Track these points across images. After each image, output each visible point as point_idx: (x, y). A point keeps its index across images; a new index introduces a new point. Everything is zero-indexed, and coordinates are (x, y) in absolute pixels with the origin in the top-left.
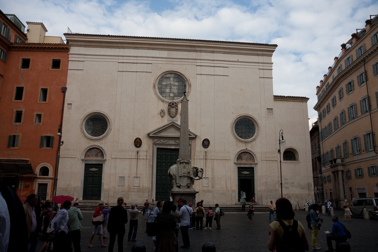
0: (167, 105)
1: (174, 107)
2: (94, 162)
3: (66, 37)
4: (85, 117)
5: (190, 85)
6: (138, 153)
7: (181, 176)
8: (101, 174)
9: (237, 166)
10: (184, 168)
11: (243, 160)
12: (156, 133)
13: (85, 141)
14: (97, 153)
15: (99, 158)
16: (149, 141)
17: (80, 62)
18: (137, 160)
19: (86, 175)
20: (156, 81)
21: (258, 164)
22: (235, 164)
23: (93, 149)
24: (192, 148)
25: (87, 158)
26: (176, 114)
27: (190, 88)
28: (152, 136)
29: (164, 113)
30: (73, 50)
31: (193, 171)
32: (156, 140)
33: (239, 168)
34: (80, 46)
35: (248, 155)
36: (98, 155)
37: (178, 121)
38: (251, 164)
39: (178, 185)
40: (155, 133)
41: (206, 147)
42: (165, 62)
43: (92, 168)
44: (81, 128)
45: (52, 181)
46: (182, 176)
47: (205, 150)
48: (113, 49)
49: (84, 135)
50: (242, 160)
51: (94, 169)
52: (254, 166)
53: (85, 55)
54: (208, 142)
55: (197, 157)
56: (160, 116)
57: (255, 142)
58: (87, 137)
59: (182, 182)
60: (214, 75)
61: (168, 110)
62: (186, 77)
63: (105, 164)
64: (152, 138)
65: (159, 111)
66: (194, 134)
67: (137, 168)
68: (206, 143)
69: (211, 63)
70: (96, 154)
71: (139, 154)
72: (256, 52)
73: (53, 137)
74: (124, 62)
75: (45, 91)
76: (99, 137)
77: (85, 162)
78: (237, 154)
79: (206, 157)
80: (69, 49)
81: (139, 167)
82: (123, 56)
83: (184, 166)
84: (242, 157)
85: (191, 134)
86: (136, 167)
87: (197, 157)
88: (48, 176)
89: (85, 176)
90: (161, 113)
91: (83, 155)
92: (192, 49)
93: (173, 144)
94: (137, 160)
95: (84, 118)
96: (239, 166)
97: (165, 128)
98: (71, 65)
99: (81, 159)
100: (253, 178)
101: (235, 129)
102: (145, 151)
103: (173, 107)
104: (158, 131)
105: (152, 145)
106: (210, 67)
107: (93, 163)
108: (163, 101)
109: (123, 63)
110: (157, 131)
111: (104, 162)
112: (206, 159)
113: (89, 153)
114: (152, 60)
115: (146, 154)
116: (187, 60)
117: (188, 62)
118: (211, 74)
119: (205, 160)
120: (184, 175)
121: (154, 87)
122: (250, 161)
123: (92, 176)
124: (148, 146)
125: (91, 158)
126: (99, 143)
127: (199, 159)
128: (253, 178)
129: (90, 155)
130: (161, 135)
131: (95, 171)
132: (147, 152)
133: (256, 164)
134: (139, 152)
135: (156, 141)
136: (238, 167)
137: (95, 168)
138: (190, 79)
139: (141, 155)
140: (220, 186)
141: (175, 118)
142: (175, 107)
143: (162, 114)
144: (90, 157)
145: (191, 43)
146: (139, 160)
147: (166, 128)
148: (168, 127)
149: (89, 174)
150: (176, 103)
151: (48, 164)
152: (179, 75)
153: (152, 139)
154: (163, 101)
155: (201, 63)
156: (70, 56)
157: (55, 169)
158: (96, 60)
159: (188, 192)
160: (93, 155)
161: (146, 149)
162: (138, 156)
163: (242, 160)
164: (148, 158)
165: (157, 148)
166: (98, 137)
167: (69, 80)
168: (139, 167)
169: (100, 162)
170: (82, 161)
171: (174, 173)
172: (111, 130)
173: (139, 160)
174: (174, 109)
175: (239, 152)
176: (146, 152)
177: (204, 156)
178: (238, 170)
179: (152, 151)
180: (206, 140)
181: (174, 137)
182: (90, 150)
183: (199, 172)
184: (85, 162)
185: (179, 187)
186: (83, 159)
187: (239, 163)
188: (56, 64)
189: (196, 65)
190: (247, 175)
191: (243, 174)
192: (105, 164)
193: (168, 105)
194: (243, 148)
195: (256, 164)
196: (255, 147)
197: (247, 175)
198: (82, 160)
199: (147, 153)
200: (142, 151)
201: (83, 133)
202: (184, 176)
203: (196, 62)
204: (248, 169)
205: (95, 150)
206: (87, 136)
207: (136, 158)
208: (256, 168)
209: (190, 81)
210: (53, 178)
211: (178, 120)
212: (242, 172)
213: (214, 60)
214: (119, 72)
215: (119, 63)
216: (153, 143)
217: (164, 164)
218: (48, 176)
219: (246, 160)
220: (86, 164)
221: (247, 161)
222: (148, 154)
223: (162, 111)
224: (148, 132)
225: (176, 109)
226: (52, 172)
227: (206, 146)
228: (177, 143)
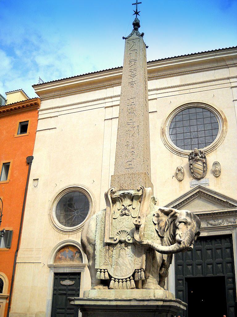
0: (186, 160)
1: (199, 160)
2: (67, 270)
3: (35, 90)
4: (55, 197)
5: (224, 121)
7: (109, 241)
8: (79, 290)
10: (125, 214)
13: (55, 234)
14: (73, 255)
15: (76, 263)
17: (52, 118)
19: (55, 292)
20: (165, 124)
23: (68, 248)
25: (58, 264)
26: (204, 171)
27: (226, 125)
29: (183, 173)
30: (44, 105)
31: (156, 222)
34: (53, 97)
36: (74, 258)
37: (210, 184)
39: (102, 277)
42: (177, 93)
43: (66, 279)
44: (50, 215)
45: (7, 302)
46: (113, 242)
48: (97, 91)
49: (54, 225)
51: (67, 282)
53: (59, 107)
56: (177, 180)
58: (56, 227)
59: (117, 264)
61: (190, 166)
62: (216, 109)
63: (84, 272)
65: (174, 171)
70: (72, 256)
73: (11, 232)
74: (113, 105)
75: (7, 166)
76: (77, 226)
77: (53, 270)
80: (38, 103)
82: (111, 97)
83: (125, 209)
88: (2, 293)
89: (54, 295)
90: (177, 174)
91: (51, 259)
92: (219, 64)
93: (204, 228)
95: (54, 199)
97: (186, 200)
98: (41, 125)
99: (48, 265)
103: (197, 160)
107: (66, 271)
108: (180, 153)
109: (112, 106)
111: (83, 269)
113: (61, 255)
116: (214, 83)
120: (123, 239)
121: (163, 133)
123: (65, 294)
125: (64, 262)
126: (75, 236)
129: (62, 257)
131: (70, 285)
137: (71, 279)
141: (202, 180)
142: (200, 160)
144: (62, 261)
145: (216, 55)
147: (188, 198)
148: (191, 197)
149: (60, 290)
150: (201, 153)
151: (3, 273)
152: (203, 108)
154: (179, 153)
156: (40, 113)
157: (11, 281)
158: (75, 111)
159: (130, 300)
160: (67, 257)
166: (74, 227)
167: (37, 145)
169: (77, 270)
170: (50, 267)
171: (88, 236)
172: (94, 213)
174: (199, 163)
181: (204, 213)
182: (62, 250)
183: (181, 226)
184: (53, 270)
185: (105, 283)
186: (51, 265)
188: (24, 128)
192: (85, 272)
193: (188, 159)
198: (50, 267)
201: (52, 222)
202: (121, 242)
203: (230, 83)
205: (71, 249)
206: (58, 226)
209: (223, 113)
210: (8, 296)
211: (209, 183)
214: (106, 121)
215: (106, 108)
217: (190, 267)
218: (2, 293)
220: (56, 274)
223: (179, 170)
225: (204, 163)
226: (7, 287)
228: (211, 225)
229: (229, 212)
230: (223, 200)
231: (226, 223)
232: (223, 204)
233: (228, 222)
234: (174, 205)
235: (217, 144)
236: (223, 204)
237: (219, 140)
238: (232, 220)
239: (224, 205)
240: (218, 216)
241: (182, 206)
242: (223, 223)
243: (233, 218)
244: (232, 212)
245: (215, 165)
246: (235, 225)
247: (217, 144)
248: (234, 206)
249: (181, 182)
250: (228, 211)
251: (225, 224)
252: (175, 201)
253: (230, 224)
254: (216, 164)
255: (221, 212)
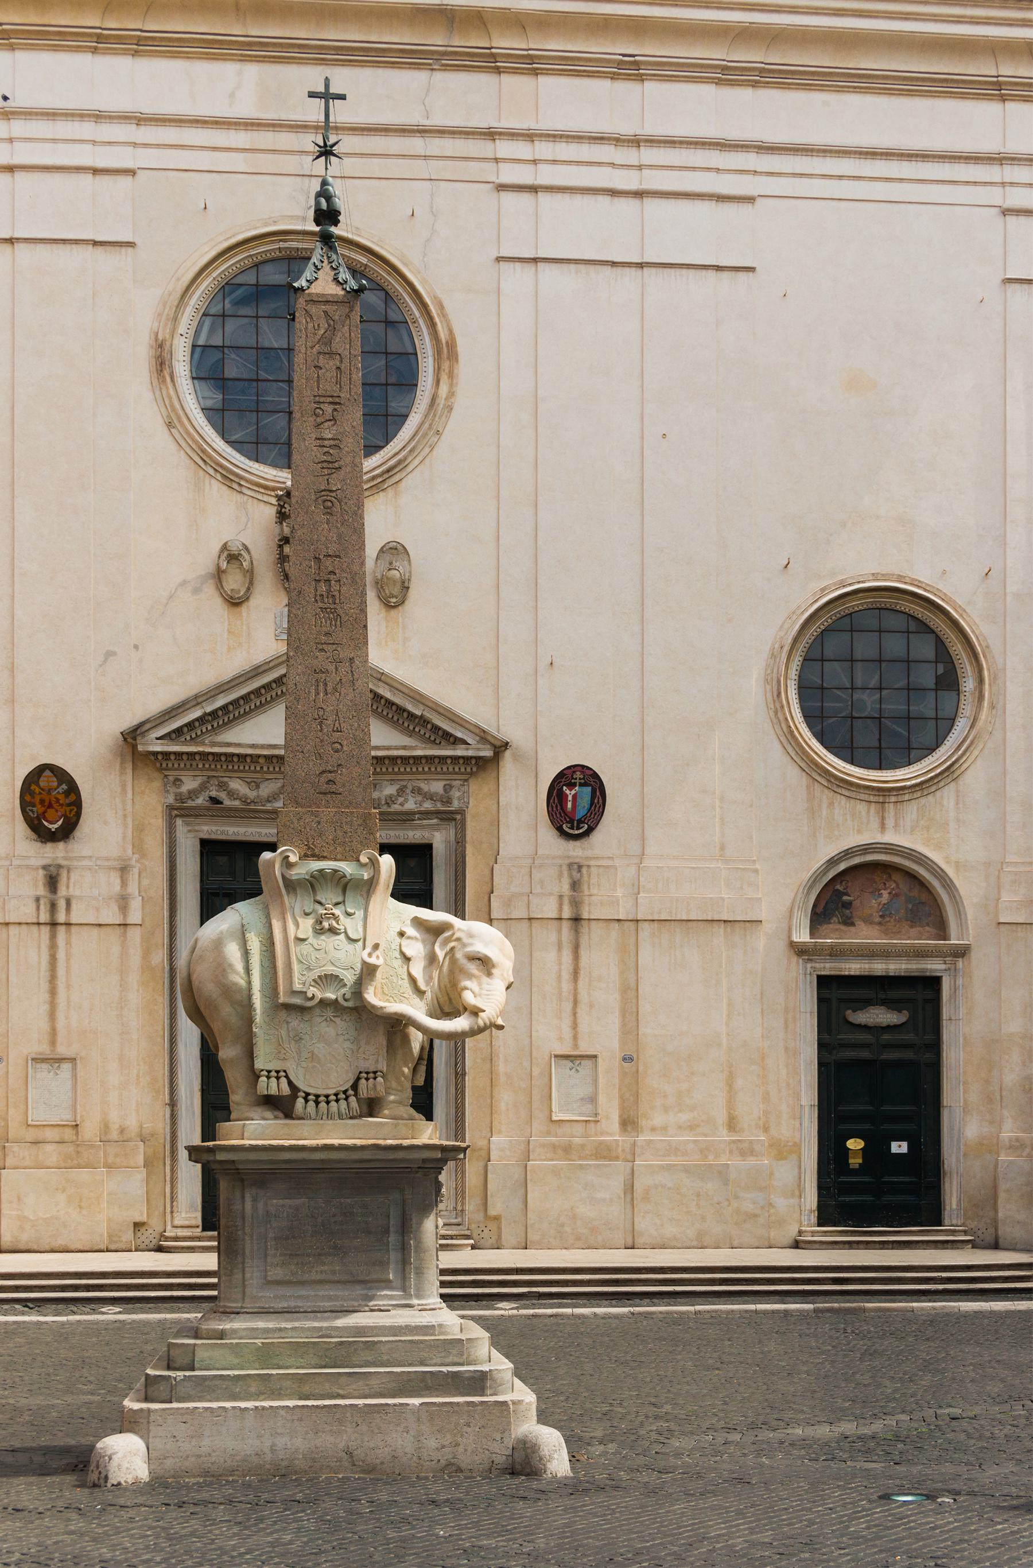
6: (52, 882)
9: (809, 965)
11: (860, 924)
12: (190, 725)
16: (143, 793)
18: (53, 937)
21: (975, 955)
22: (800, 951)
24: (468, 838)
28: (158, 749)
32: (189, 784)
33: (823, 982)
35: (898, 883)
38: (921, 954)
40: (179, 731)
41: (578, 828)
47: (571, 853)
50: (853, 924)
52: (943, 967)
54: (594, 792)
55: (508, 903)
57: (957, 791)
60: (641, 265)
61: (280, 546)
64: (161, 769)
66: (483, 736)
67: (53, 992)
68: (575, 797)
69: (613, 165)
71: (62, 891)
72: (983, 68)
78: (811, 887)
79: (576, 904)
81: (68, 987)
84: (848, 905)
85: (459, 735)
86: (45, 986)
87: (508, 903)
94: (53, 937)
96: (829, 967)
97: (257, 692)
100: (928, 1056)
101: (804, 689)
102: (110, 868)
104: (206, 714)
105: (158, 822)
106: (604, 200)
110: (197, 713)
112: (576, 920)
114: (135, 145)
115: (117, 888)
117: (426, 157)
118: (616, 260)
119: (566, 926)
122: (913, 932)
124: (130, 831)
127: (525, 924)
128: (928, 1056)
130: (229, 745)
132: (124, 870)
133: (961, 952)
134: (64, 874)
135: (190, 792)
136: (819, 977)
138: (445, 303)
139: (80, 898)
140: (684, 1117)
143: (234, 582)
146: (68, 932)
153: (156, 774)
155: (531, 167)
161: (114, 851)
162: (53, 907)
163: (848, 922)
164: (135, 916)
165: (205, 843)
168: (68, 987)
173: (68, 932)
175: (832, 862)
176: (118, 874)
177: (566, 901)
178: (820, 1000)
179: (161, 870)
180: (578, 775)
187: (832, 947)
189: (493, 179)
190: (886, 1037)
191: (859, 1026)
194: (859, 832)
195: (961, 952)
196: (952, 825)
197: (886, 1037)
199: (124, 883)
200: (86, 863)
204: (895, 994)
207: (44, 917)
208: (960, 981)
212: (849, 1012)
213: (636, 142)
216: (170, 808)
219: (880, 923)
221: (886, 934)
222: (133, 888)
224: (128, 721)
227: (580, 821)
229: (430, 759)
230: (410, 707)
231: (410, 797)
232: (406, 724)
233: (420, 798)
234: (209, 709)
235: (405, 458)
236: (406, 724)
237: (413, 444)
238: (437, 787)
239: (411, 728)
240: (384, 770)
241: (240, 716)
242: (401, 800)
243: (441, 784)
244: (443, 759)
245: (388, 557)
246: (445, 812)
247: (405, 458)
248: (452, 739)
249: (238, 609)
250: (426, 757)
251: (410, 805)
252: (212, 693)
253: (428, 805)
254: (394, 551)
255: (397, 757)
